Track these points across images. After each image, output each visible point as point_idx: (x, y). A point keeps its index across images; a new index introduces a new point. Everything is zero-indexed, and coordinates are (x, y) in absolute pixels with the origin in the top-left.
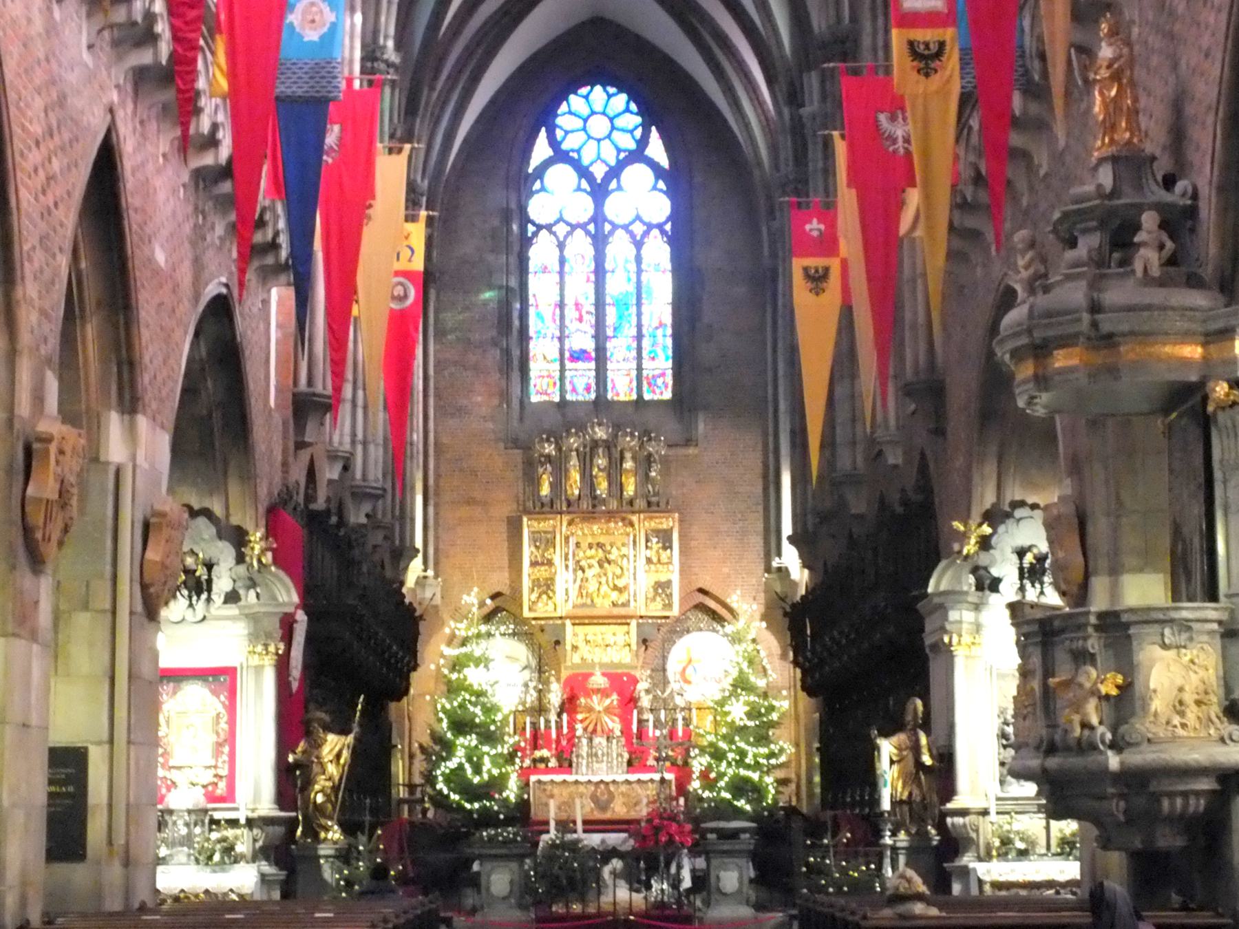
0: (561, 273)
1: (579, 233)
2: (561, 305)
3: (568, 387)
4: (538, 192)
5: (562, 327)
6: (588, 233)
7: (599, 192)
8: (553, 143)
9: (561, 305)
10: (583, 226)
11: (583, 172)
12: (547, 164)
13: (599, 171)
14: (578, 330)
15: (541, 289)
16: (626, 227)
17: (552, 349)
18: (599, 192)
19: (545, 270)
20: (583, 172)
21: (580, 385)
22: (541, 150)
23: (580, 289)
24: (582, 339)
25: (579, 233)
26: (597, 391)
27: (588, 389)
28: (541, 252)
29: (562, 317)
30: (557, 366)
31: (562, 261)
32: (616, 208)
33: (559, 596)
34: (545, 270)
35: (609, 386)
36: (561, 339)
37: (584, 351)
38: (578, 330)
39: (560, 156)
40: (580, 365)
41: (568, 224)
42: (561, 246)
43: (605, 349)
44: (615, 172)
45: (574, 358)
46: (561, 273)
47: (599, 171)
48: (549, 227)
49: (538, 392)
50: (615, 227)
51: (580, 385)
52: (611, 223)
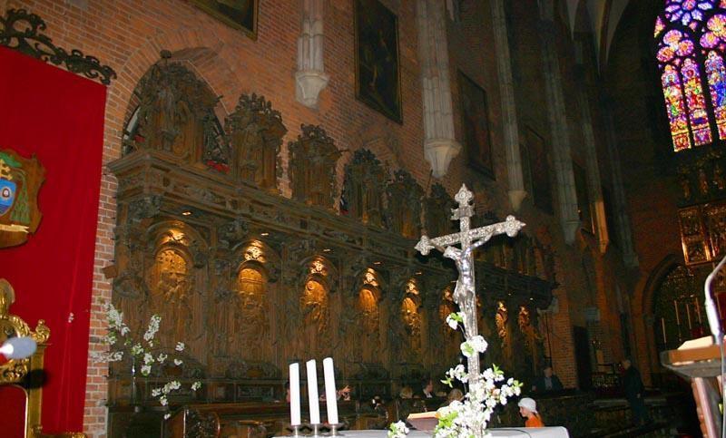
0: (681, 83)
1: (688, 60)
2: (684, 98)
3: (695, 138)
4: (661, 47)
5: (687, 109)
6: (692, 58)
7: (694, 35)
8: (666, 22)
9: (684, 98)
10: (689, 56)
11: (684, 29)
12: (663, 33)
13: (693, 26)
14: (695, 109)
15: (672, 93)
16: (715, 48)
17: (682, 122)
18: (694, 35)
19: (671, 84)
20: (684, 29)
21: (702, 135)
22: (659, 27)
23: (694, 87)
24: (701, 114)
25: (688, 60)
26: (713, 138)
27: (706, 137)
28: (669, 75)
29: (686, 104)
30: (687, 130)
31: (680, 76)
32: (708, 40)
33: (707, 253)
34: (671, 84)
35: (720, 132)
36: (687, 115)
37: (701, 119)
38: (695, 109)
39: (669, 26)
40: (700, 126)
41: (680, 57)
42: (678, 69)
43: (714, 114)
44: (702, 24)
45: (696, 124)
46: (681, 83)
47: (693, 26)
48: (671, 62)
49: (678, 147)
50: (708, 50)
51: (702, 135)
52: (704, 49)
